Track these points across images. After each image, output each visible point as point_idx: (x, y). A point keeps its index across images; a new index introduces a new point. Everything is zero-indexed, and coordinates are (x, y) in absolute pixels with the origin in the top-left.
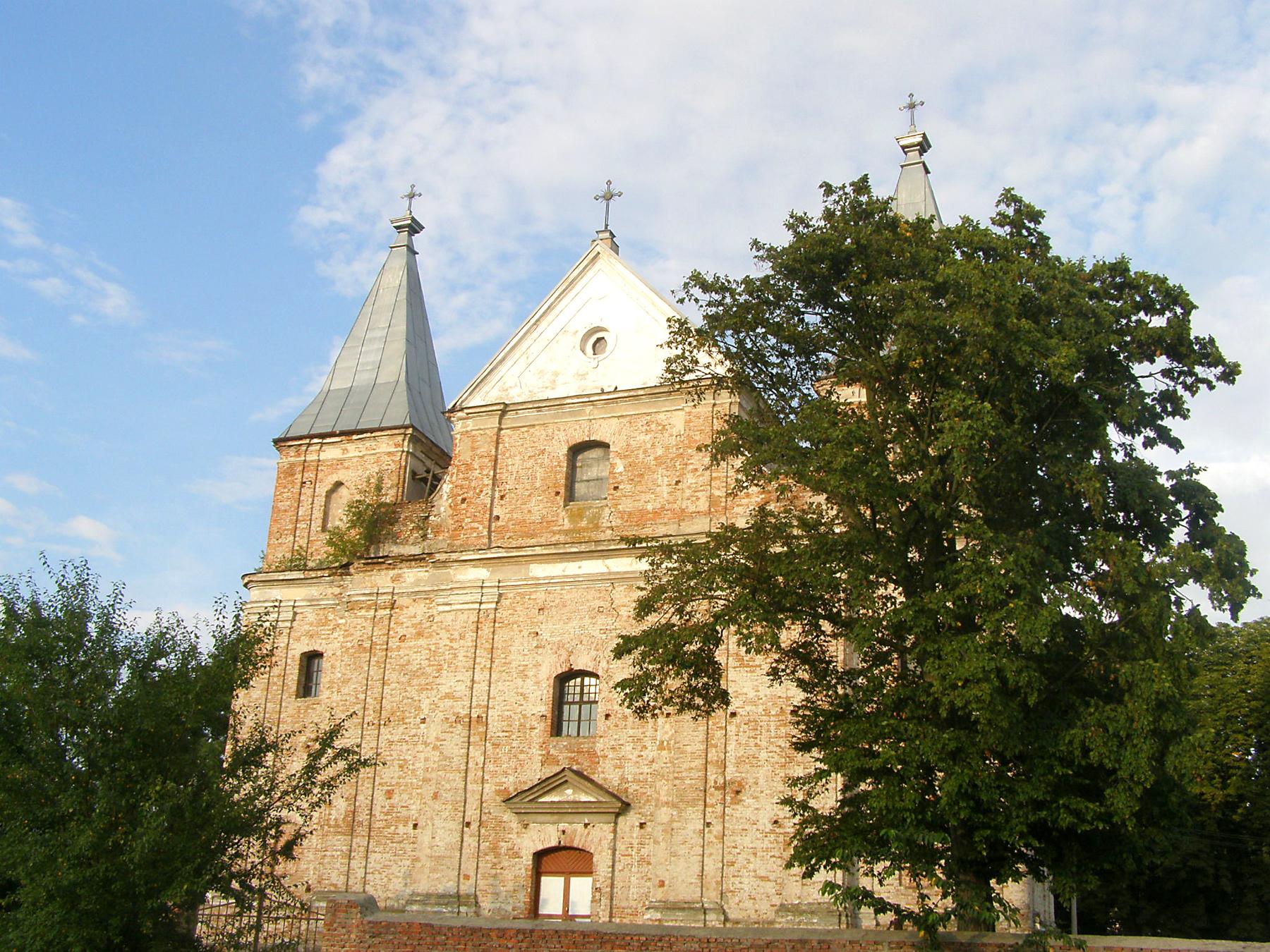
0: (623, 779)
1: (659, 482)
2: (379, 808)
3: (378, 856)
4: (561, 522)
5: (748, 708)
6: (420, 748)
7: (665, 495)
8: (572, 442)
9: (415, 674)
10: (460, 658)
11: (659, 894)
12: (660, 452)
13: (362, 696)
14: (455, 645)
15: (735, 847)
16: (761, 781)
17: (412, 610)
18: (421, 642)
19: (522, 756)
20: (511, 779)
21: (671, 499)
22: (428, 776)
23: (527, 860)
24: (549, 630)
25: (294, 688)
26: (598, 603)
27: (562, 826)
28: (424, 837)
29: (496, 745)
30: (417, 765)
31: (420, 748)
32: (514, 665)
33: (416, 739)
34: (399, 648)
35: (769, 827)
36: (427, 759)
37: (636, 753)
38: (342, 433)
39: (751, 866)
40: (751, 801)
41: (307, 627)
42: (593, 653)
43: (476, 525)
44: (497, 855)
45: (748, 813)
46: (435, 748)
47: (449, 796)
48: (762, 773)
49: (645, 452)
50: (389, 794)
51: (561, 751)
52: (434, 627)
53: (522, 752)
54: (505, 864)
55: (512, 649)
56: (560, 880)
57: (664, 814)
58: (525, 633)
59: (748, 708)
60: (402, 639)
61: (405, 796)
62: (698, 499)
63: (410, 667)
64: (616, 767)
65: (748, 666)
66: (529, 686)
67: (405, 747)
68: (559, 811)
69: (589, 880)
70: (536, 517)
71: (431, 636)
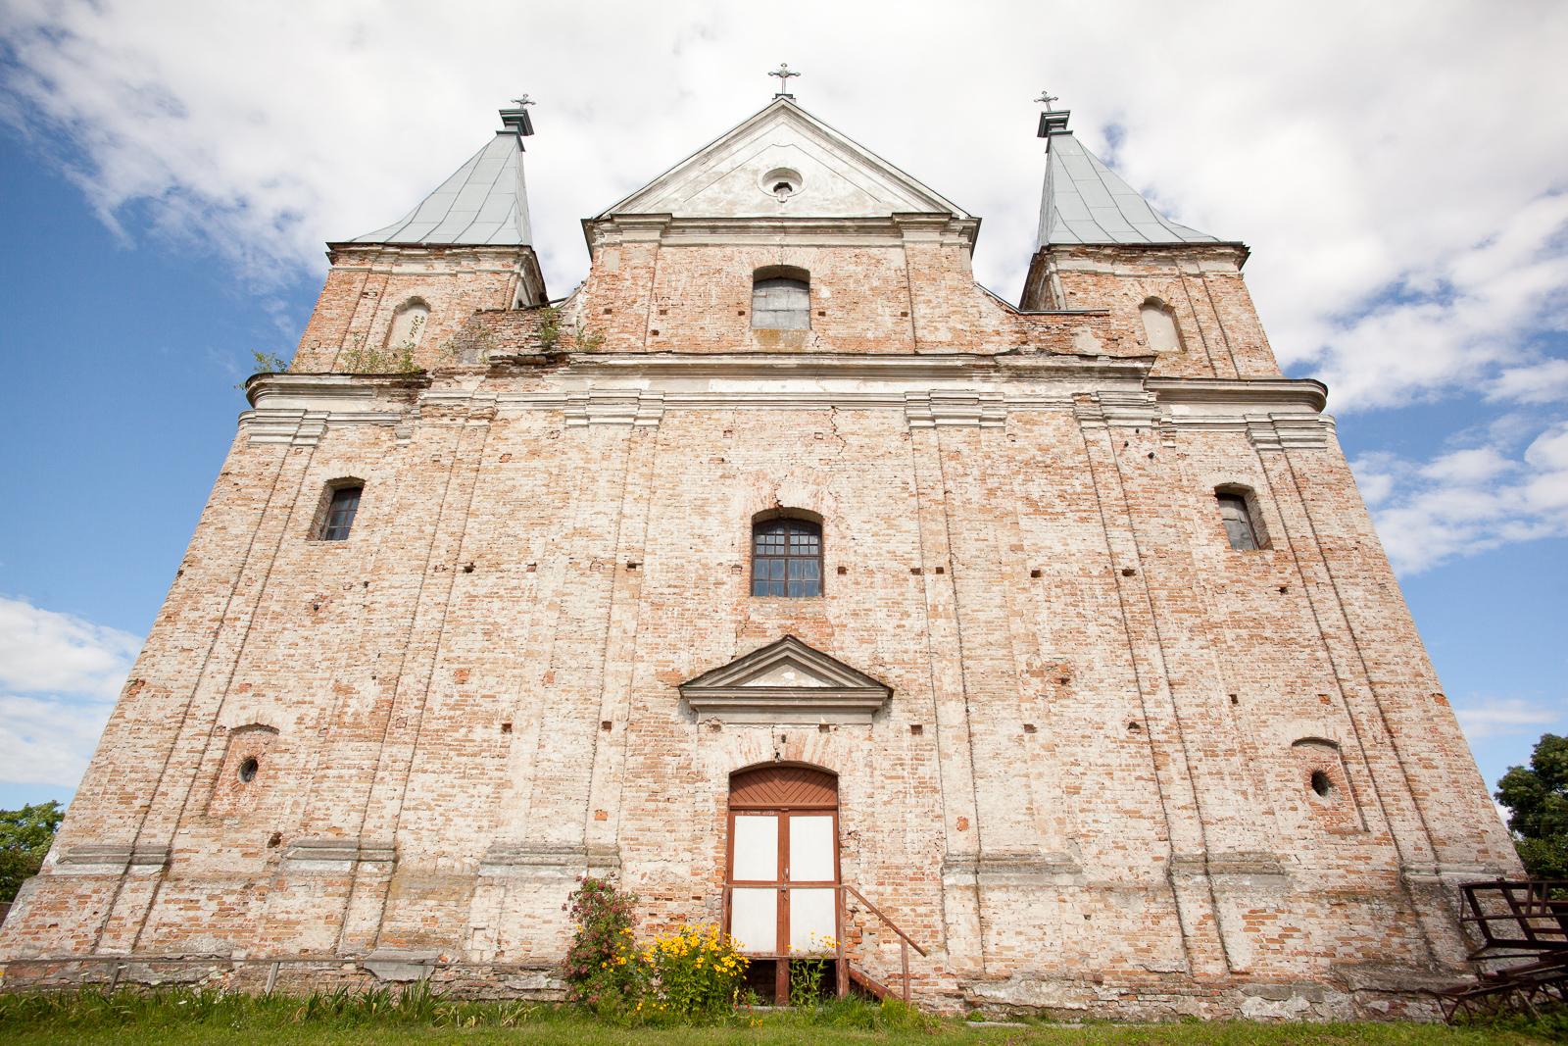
1: (880, 311)
2: (439, 697)
3: (429, 778)
4: (748, 342)
5: (1057, 566)
6: (524, 606)
7: (890, 325)
8: (757, 266)
9: (522, 504)
10: (602, 482)
11: (959, 843)
12: (876, 283)
13: (429, 529)
14: (593, 467)
15: (1076, 763)
16: (1098, 665)
17: (524, 425)
18: (536, 463)
19: (701, 623)
20: (685, 656)
21: (898, 329)
22: (536, 647)
24: (736, 457)
25: (307, 525)
26: (814, 429)
27: (779, 730)
28: (523, 745)
29: (657, 606)
30: (517, 632)
31: (524, 606)
32: (686, 497)
33: (518, 593)
34: (498, 470)
35: (1124, 733)
36: (534, 623)
37: (895, 622)
38: (428, 246)
39: (1108, 795)
40: (1088, 694)
41: (343, 448)
42: (812, 488)
43: (626, 336)
44: (659, 778)
45: (1088, 712)
46: (551, 606)
47: (575, 680)
48: (1098, 654)
49: (857, 282)
50: (462, 676)
51: (772, 618)
52: (559, 446)
53: (702, 616)
54: (673, 792)
55: (684, 478)
56: (771, 822)
57: (952, 713)
58: (705, 459)
59: (1057, 566)
60: (506, 458)
61: (491, 680)
62: (936, 329)
63: (515, 495)
64: (862, 641)
65: (1045, 513)
66: (712, 525)
67: (497, 604)
68: (777, 705)
69: (825, 822)
70: (712, 334)
71: (553, 455)
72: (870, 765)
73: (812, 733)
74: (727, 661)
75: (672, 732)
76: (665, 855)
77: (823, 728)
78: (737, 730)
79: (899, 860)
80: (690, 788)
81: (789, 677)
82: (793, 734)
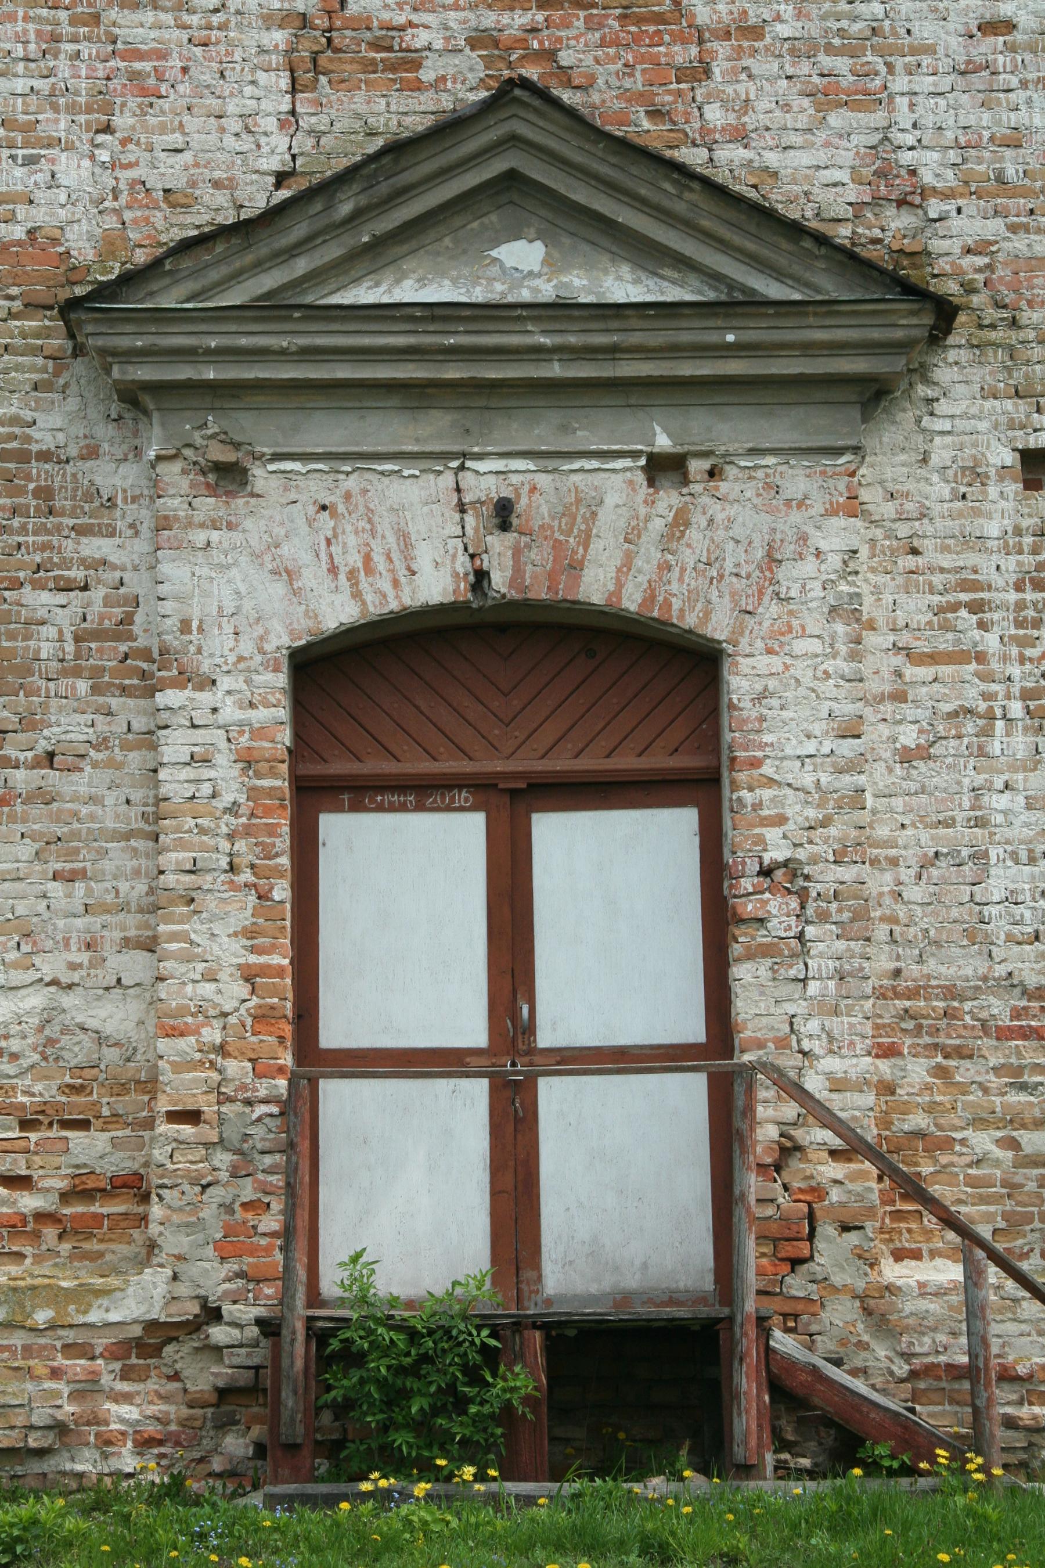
0: (894, 185)
20: (74, 170)
23: (253, 704)
27: (485, 480)
54: (69, 727)
56: (461, 837)
64: (826, 97)
68: (472, 379)
69: (676, 827)
72: (846, 610)
73: (617, 490)
74: (258, 198)
75: (45, 493)
76: (49, 966)
77: (664, 468)
78: (317, 487)
79: (962, 966)
80: (129, 711)
81: (523, 265)
82: (540, 491)
